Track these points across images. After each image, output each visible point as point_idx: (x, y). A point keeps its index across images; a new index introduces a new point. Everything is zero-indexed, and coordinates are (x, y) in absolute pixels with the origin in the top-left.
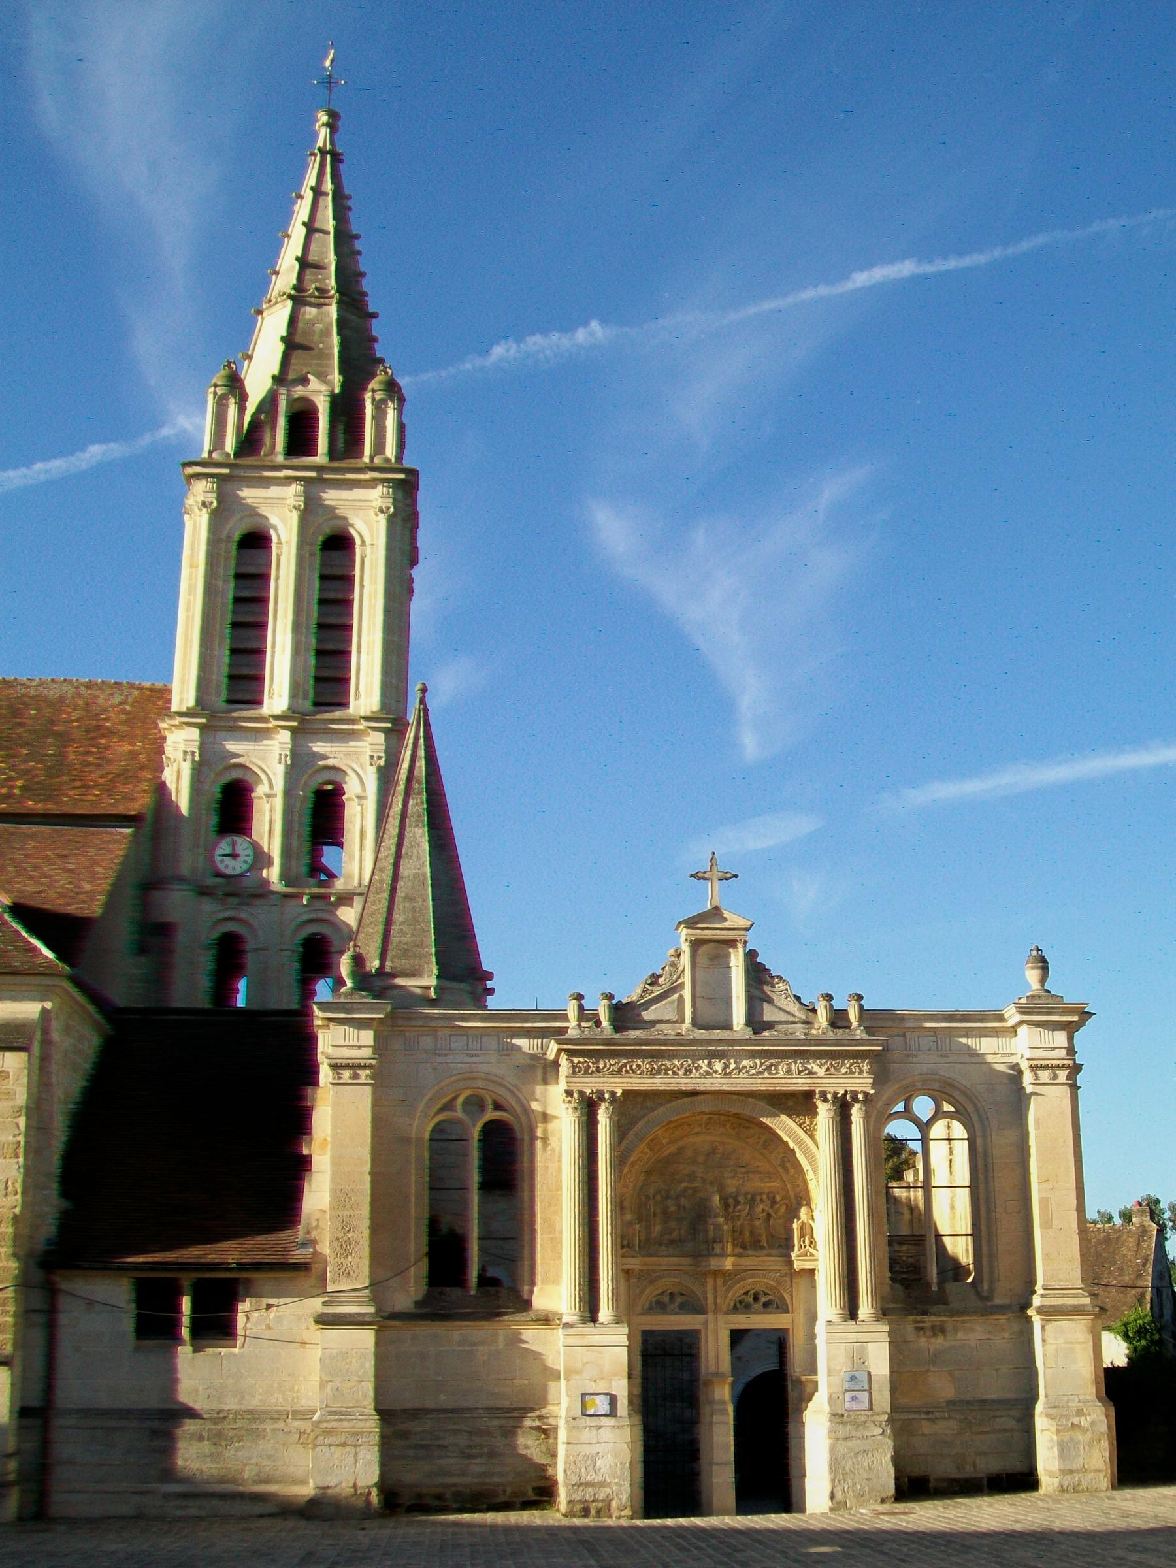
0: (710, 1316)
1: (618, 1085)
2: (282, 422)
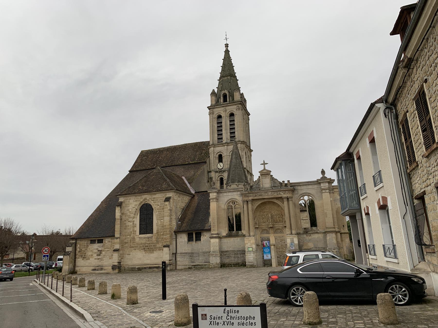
1: (251, 198)
2: (222, 98)
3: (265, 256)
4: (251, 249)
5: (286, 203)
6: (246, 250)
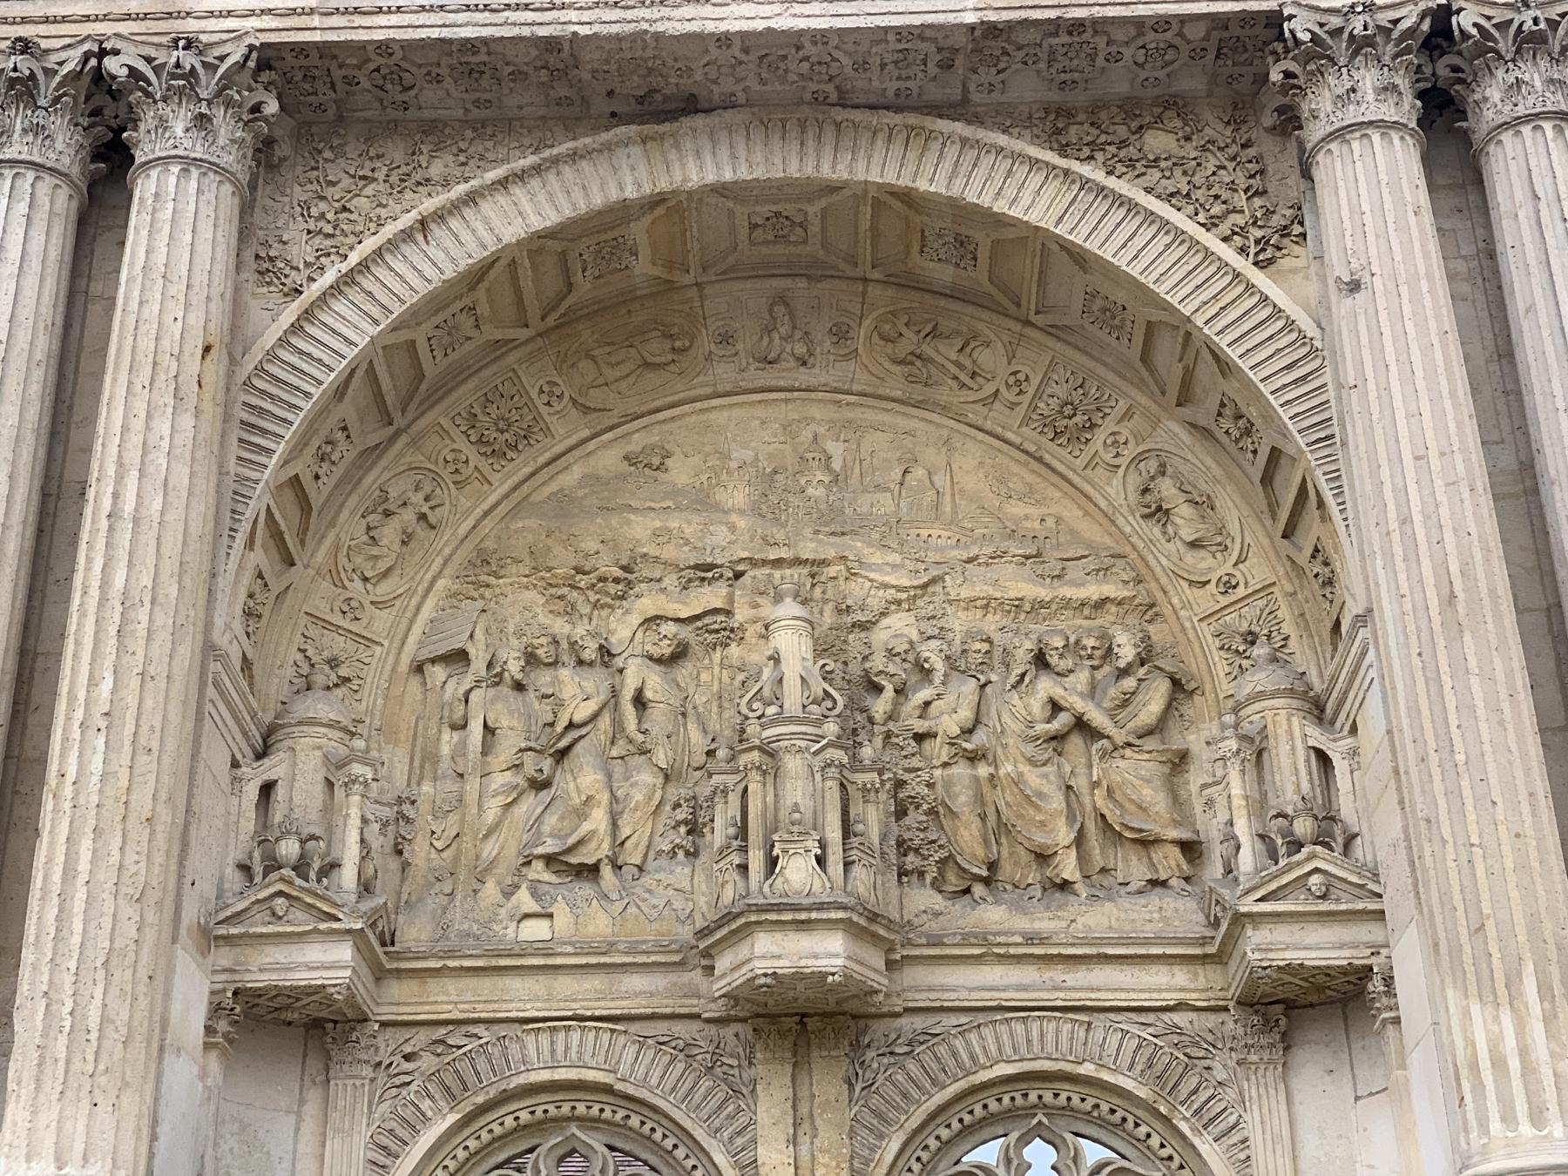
5: (1371, 184)
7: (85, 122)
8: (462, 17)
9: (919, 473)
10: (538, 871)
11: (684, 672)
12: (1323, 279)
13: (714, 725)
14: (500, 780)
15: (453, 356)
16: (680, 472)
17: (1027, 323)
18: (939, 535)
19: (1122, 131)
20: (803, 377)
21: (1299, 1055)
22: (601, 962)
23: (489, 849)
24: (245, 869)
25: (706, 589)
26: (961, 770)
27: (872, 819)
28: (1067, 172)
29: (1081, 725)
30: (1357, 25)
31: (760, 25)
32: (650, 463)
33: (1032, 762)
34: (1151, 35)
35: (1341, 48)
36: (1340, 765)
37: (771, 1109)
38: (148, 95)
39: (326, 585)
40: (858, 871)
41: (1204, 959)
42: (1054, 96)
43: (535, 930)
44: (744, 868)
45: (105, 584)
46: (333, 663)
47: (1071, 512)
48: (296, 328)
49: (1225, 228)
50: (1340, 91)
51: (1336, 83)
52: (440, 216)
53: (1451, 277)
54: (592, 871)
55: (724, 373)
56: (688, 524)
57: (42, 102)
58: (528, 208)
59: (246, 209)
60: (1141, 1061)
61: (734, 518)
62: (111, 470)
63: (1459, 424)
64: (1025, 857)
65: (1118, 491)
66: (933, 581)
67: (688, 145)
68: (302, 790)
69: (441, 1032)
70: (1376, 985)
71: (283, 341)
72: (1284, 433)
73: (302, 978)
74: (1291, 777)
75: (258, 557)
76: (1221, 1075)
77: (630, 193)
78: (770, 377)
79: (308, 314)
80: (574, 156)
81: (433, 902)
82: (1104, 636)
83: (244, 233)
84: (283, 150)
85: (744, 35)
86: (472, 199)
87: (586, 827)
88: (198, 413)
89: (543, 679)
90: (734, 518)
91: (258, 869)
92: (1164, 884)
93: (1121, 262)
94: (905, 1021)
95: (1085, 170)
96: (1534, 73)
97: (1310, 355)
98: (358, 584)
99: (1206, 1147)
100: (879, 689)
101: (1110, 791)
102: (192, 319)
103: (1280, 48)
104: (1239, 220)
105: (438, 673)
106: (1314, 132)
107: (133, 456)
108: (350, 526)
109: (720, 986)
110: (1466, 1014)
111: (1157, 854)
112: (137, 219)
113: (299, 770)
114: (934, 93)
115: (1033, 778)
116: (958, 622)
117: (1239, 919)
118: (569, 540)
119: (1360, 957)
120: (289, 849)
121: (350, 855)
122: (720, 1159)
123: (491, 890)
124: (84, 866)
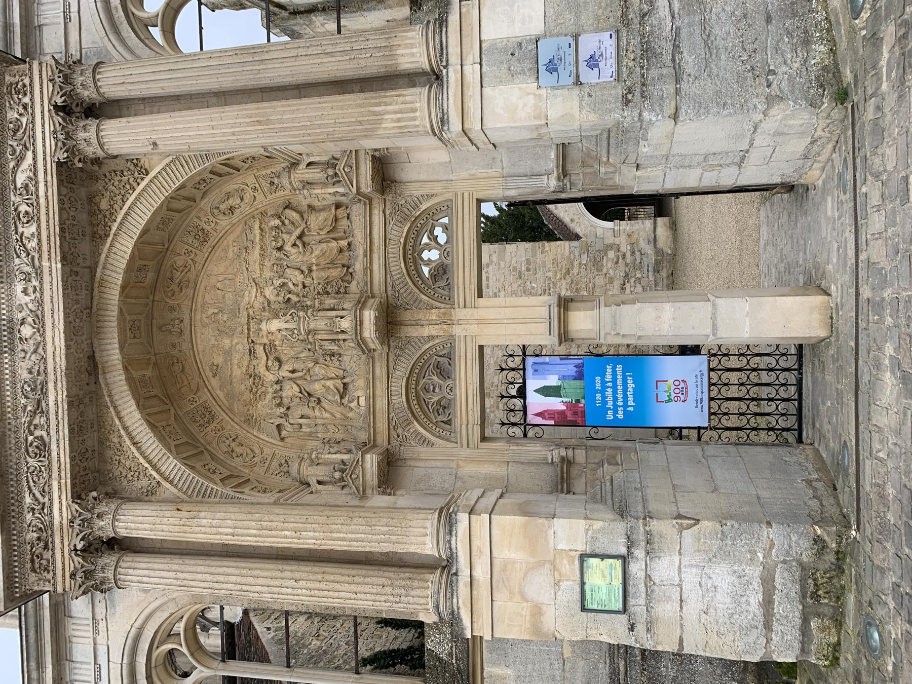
0: (457, 331)
1: (61, 507)
3: (675, 414)
4: (603, 580)
5: (119, 136)
6: (614, 632)
7: (100, 554)
8: (61, 434)
9: (219, 285)
10: (345, 401)
11: (284, 358)
12: (152, 154)
13: (300, 349)
14: (317, 413)
15: (180, 432)
16: (219, 360)
17: (167, 249)
18: (239, 279)
19: (100, 216)
20: (187, 321)
21: (397, 178)
22: (372, 382)
23: (338, 415)
24: (343, 487)
25: (257, 351)
26: (314, 274)
27: (329, 302)
28: (115, 235)
29: (300, 237)
30: (61, 137)
31: (62, 335)
32: (216, 370)
33: (311, 253)
34: (65, 205)
35: (70, 143)
36: (312, 159)
37: (413, 332)
38: (90, 534)
39: (255, 469)
40: (345, 306)
41: (370, 204)
42: (88, 238)
43: (362, 401)
44: (344, 340)
45: (255, 536)
46: (281, 465)
47: (231, 238)
48: (171, 482)
49: (135, 184)
50: (85, 144)
51: (83, 145)
52: (131, 438)
53: (151, 113)
54: (344, 384)
55: (185, 346)
56: (236, 358)
57: (93, 568)
58: (129, 410)
59: (130, 500)
60: (400, 225)
61: (234, 343)
62: (218, 537)
63: (201, 114)
64: (341, 256)
65: (225, 222)
66: (254, 281)
67: (106, 359)
68: (321, 472)
69: (391, 427)
70: (377, 154)
71: (175, 486)
72: (205, 169)
73: (375, 469)
74: (315, 174)
75: (247, 490)
76: (404, 201)
77: (123, 377)
78: (187, 332)
79: (166, 479)
80: (110, 396)
81: (354, 431)
82: (272, 228)
83: (139, 500)
84: (109, 489)
85: (66, 341)
86: (126, 429)
87: (332, 387)
88: (199, 511)
89: (286, 401)
90: (234, 343)
91: (343, 484)
92: (348, 215)
93: (146, 218)
94: (389, 293)
95: (114, 229)
96: (79, 80)
97: (178, 159)
98: (255, 459)
99: (423, 207)
100: (289, 299)
101: (321, 229)
102: (168, 515)
103: (69, 163)
104: (131, 180)
105: (284, 433)
106: (100, 153)
107: (214, 530)
108: (237, 462)
109: (379, 347)
110: (385, 128)
111: (340, 216)
112: (134, 534)
113: (313, 473)
114: (87, 278)
115: (316, 253)
116: (268, 274)
117: (358, 193)
118: (241, 394)
119: (369, 158)
120: (337, 475)
121: (339, 457)
122: (427, 347)
123: (350, 415)
124: (341, 535)
